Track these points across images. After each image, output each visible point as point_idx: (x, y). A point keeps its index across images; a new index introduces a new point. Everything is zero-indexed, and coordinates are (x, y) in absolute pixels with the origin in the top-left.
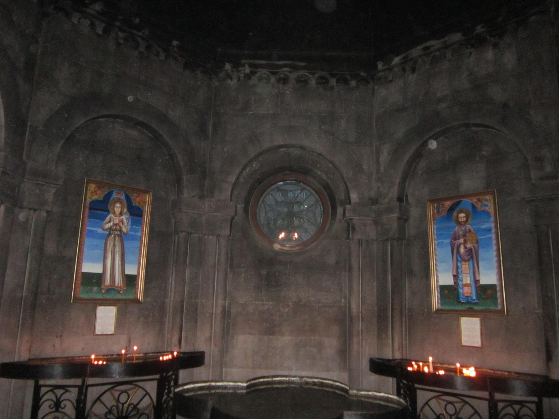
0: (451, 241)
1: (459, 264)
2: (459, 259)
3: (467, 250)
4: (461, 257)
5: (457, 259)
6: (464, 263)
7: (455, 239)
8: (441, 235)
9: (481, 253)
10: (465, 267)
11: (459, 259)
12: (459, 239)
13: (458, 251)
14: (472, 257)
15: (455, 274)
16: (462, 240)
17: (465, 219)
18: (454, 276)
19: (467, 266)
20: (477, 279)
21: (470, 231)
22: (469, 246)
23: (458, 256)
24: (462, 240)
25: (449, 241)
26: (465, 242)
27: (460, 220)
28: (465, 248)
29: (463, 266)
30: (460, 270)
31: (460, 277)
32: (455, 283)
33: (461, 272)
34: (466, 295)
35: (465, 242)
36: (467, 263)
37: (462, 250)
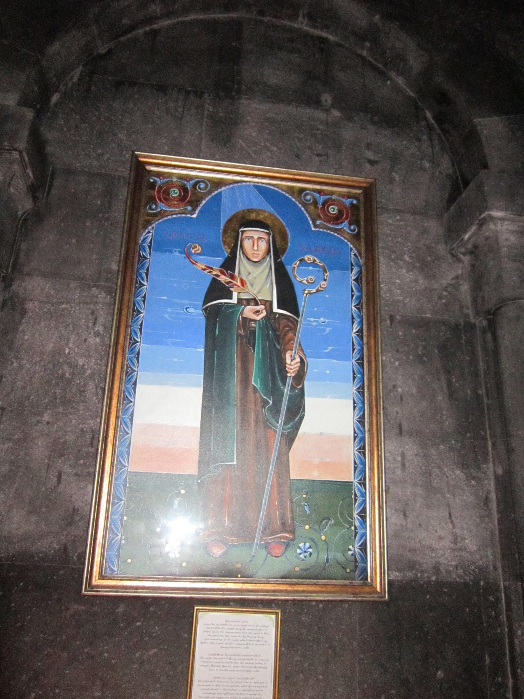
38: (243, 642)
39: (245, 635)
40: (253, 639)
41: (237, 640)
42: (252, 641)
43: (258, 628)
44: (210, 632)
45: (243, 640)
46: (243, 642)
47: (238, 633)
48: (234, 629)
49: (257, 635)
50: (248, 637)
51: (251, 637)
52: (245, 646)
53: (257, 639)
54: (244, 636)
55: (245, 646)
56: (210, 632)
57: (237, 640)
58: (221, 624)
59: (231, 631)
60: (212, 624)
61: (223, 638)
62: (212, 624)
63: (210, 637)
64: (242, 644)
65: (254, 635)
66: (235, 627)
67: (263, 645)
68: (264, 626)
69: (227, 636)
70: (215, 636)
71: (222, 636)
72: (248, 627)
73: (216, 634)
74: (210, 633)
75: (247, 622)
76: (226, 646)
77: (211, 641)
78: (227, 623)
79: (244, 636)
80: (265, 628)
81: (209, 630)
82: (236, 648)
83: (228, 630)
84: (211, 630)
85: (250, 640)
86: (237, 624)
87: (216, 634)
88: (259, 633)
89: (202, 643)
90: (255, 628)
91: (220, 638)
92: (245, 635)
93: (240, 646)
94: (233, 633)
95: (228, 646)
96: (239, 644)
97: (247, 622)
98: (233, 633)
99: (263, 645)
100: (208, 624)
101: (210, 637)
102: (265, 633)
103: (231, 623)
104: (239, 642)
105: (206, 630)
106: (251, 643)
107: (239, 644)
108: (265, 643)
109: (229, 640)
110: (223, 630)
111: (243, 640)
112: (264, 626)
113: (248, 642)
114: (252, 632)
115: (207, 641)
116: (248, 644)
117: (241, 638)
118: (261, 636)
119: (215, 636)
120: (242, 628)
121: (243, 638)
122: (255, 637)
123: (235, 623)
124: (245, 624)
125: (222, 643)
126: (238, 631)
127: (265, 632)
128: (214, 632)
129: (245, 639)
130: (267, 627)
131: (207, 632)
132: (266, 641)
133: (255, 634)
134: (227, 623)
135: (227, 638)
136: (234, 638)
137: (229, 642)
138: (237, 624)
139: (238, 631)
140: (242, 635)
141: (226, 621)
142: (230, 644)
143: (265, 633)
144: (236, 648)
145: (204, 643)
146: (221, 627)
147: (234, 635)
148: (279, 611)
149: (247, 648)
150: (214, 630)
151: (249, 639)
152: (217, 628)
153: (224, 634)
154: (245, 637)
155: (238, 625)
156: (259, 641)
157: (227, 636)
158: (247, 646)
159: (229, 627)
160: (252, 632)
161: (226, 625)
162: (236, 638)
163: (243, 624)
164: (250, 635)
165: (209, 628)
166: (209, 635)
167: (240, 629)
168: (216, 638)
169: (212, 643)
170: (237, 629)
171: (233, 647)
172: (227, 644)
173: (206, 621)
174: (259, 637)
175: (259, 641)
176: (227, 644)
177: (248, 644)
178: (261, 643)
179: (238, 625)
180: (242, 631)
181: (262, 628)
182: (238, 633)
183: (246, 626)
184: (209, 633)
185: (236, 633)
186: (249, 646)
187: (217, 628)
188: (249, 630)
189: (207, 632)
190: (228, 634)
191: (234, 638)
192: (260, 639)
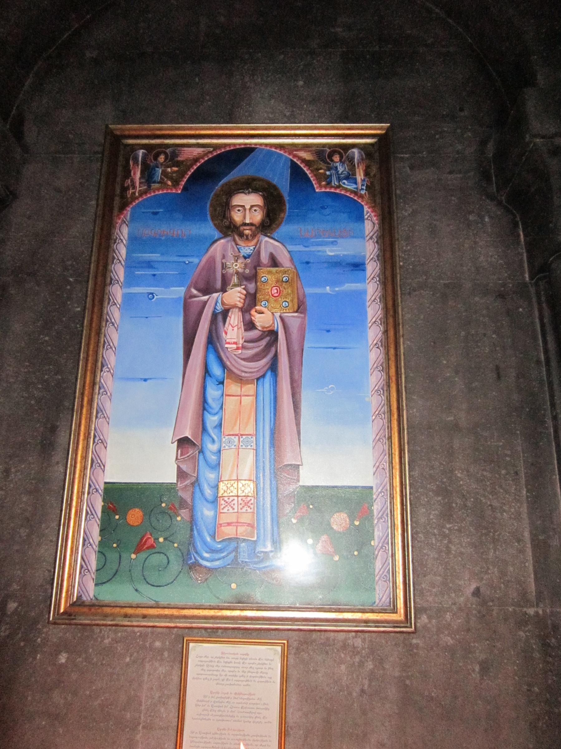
0: (189, 296)
1: (213, 392)
2: (216, 370)
3: (253, 334)
4: (224, 366)
5: (207, 372)
6: (233, 388)
7: (207, 290)
8: (149, 265)
9: (316, 356)
10: (239, 404)
11: (216, 370)
12: (223, 290)
13: (213, 340)
14: (274, 367)
15: (188, 434)
16: (235, 295)
17: (258, 217)
18: (183, 443)
19: (247, 401)
20: (289, 459)
21: (274, 262)
22: (263, 319)
23: (212, 358)
24: (235, 295)
25: (180, 291)
26: (252, 300)
27: (237, 217)
28: (250, 325)
29: (230, 403)
30: (211, 420)
31: (211, 447)
32: (181, 474)
33: (220, 425)
34: (229, 531)
35: (252, 300)
36: (250, 388)
37: (233, 333)
38: (242, 679)
39: (245, 669)
40: (254, 675)
41: (236, 676)
42: (254, 677)
44: (203, 665)
45: (243, 676)
46: (242, 679)
47: (237, 667)
48: (231, 662)
49: (260, 670)
50: (249, 672)
51: (252, 673)
52: (245, 683)
53: (259, 675)
54: (243, 672)
55: (245, 683)
56: (203, 665)
57: (236, 676)
58: (216, 657)
59: (227, 665)
60: (206, 656)
62: (206, 656)
63: (202, 672)
64: (242, 681)
65: (255, 670)
66: (233, 661)
67: (267, 682)
68: (267, 660)
69: (223, 670)
70: (210, 671)
71: (217, 671)
72: (247, 661)
73: (210, 668)
74: (205, 668)
75: (247, 655)
76: (223, 683)
77: (205, 677)
78: (223, 656)
79: (243, 672)
81: (202, 664)
82: (234, 684)
83: (224, 664)
84: (205, 664)
85: (250, 677)
86: (236, 656)
87: (210, 668)
88: (262, 669)
89: (193, 678)
90: (257, 662)
91: (215, 673)
92: (245, 669)
93: (240, 683)
94: (230, 667)
95: (225, 682)
96: (238, 681)
97: (247, 655)
98: (230, 667)
99: (267, 682)
100: (201, 657)
101: (202, 672)
102: (270, 668)
104: (238, 678)
105: (199, 663)
106: (252, 679)
107: (238, 681)
108: (269, 680)
109: (226, 675)
110: (219, 664)
111: (243, 676)
112: (267, 660)
113: (248, 678)
114: (253, 666)
115: (200, 676)
116: (247, 681)
117: (241, 674)
118: (263, 670)
119: (210, 671)
120: (242, 661)
121: (243, 673)
122: (257, 673)
123: (233, 656)
124: (245, 657)
125: (219, 679)
127: (270, 666)
128: (208, 666)
129: (245, 674)
130: (272, 660)
131: (201, 666)
132: (271, 678)
133: (257, 669)
134: (223, 656)
135: (223, 673)
136: (231, 674)
138: (236, 656)
140: (241, 670)
142: (227, 680)
143: (270, 668)
144: (234, 684)
145: (197, 679)
146: (216, 660)
147: (232, 669)
148: (285, 642)
149: (247, 685)
150: (207, 663)
151: (250, 674)
152: (211, 661)
154: (245, 672)
155: (237, 659)
156: (262, 677)
157: (223, 670)
158: (247, 683)
159: (226, 660)
160: (253, 666)
161: (222, 657)
162: (234, 673)
163: (242, 657)
164: (251, 670)
165: (202, 661)
166: (202, 670)
167: (239, 663)
168: (211, 673)
169: (206, 678)
170: (235, 663)
171: (231, 685)
172: (223, 680)
173: (199, 652)
174: (261, 672)
175: (262, 677)
176: (223, 680)
177: (247, 681)
179: (237, 659)
180: (241, 665)
181: (266, 662)
182: (237, 667)
183: (246, 659)
184: (202, 668)
185: (234, 667)
186: (249, 683)
187: (211, 661)
188: (249, 664)
189: (201, 666)
190: (224, 668)
191: (231, 674)
192: (263, 675)
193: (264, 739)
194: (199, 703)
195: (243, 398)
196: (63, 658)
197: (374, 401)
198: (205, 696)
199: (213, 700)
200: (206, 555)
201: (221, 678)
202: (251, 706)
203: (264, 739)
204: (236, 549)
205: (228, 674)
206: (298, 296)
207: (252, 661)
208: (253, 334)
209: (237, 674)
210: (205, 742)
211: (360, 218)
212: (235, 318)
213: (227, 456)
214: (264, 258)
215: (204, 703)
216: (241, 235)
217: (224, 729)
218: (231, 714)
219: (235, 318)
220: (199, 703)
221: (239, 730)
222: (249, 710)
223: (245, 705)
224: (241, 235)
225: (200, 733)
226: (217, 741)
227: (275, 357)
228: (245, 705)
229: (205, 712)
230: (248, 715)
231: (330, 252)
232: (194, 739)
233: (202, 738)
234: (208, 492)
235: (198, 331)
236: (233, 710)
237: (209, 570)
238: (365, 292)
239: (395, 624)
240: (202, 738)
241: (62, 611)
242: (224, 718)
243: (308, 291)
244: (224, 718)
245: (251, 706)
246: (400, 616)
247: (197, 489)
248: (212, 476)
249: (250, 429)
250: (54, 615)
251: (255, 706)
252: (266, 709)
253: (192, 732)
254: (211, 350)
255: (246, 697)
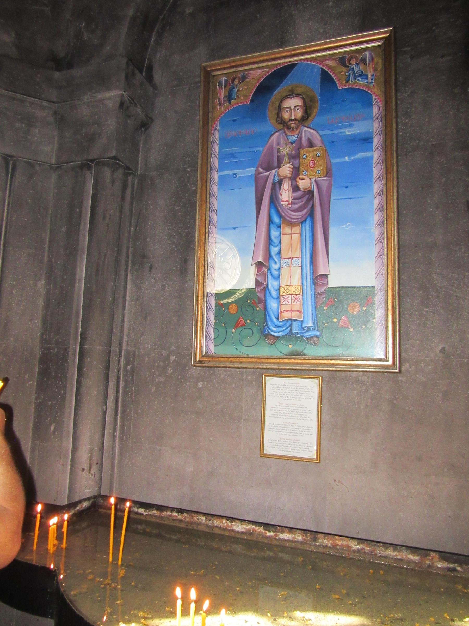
0: (258, 173)
1: (274, 233)
2: (276, 219)
3: (298, 194)
4: (280, 216)
5: (270, 220)
6: (287, 230)
7: (269, 168)
8: (232, 155)
9: (338, 204)
10: (291, 240)
11: (276, 219)
12: (279, 167)
13: (274, 200)
14: (311, 214)
15: (261, 259)
16: (286, 170)
17: (299, 114)
18: (259, 265)
19: (296, 237)
20: (321, 271)
21: (311, 144)
22: (303, 184)
23: (273, 212)
24: (286, 170)
25: (251, 171)
26: (296, 172)
27: (286, 116)
28: (296, 188)
29: (285, 239)
30: (274, 250)
31: (275, 267)
32: (258, 283)
33: (279, 253)
34: (287, 316)
35: (296, 172)
36: (297, 229)
37: (286, 194)
43: (306, 388)
52: (298, 399)
55: (298, 399)
59: (288, 389)
60: (276, 385)
61: (283, 393)
63: (274, 393)
66: (291, 387)
67: (310, 399)
72: (299, 387)
75: (298, 384)
80: (311, 388)
91: (280, 393)
93: (295, 399)
97: (298, 384)
99: (310, 399)
101: (274, 393)
103: (288, 384)
104: (294, 396)
105: (272, 388)
116: (299, 398)
120: (296, 387)
126: (293, 389)
135: (285, 393)
136: (290, 394)
137: (287, 396)
139: (293, 389)
140: (295, 392)
141: (285, 383)
146: (281, 386)
147: (290, 391)
153: (284, 391)
177: (299, 398)
178: (308, 397)
191: (290, 394)
193: (309, 428)
194: (272, 409)
195: (293, 235)
196: (200, 385)
197: (376, 232)
198: (276, 405)
199: (280, 407)
200: (274, 329)
201: (284, 396)
202: (302, 411)
203: (309, 428)
204: (291, 326)
205: (288, 394)
206: (327, 165)
207: (301, 387)
208: (298, 194)
209: (293, 394)
210: (277, 429)
211: (370, 105)
212: (286, 185)
213: (284, 272)
214: (304, 141)
215: (275, 409)
216: (289, 128)
217: (287, 423)
218: (290, 415)
219: (286, 185)
220: (272, 409)
221: (295, 423)
222: (299, 413)
223: (298, 411)
224: (289, 128)
225: (274, 424)
226: (283, 428)
227: (313, 207)
228: (298, 411)
229: (276, 414)
230: (300, 416)
231: (348, 132)
232: (271, 427)
233: (275, 426)
234: (274, 293)
235: (265, 195)
236: (292, 413)
237: (277, 338)
238: (372, 158)
239: (387, 367)
240: (275, 426)
241: (198, 360)
242: (287, 417)
243: (334, 161)
244: (287, 417)
245: (302, 411)
246: (390, 362)
247: (268, 292)
248: (275, 284)
249: (298, 254)
250: (194, 362)
251: (304, 411)
252: (310, 413)
253: (269, 424)
254: (273, 206)
255: (298, 406)
